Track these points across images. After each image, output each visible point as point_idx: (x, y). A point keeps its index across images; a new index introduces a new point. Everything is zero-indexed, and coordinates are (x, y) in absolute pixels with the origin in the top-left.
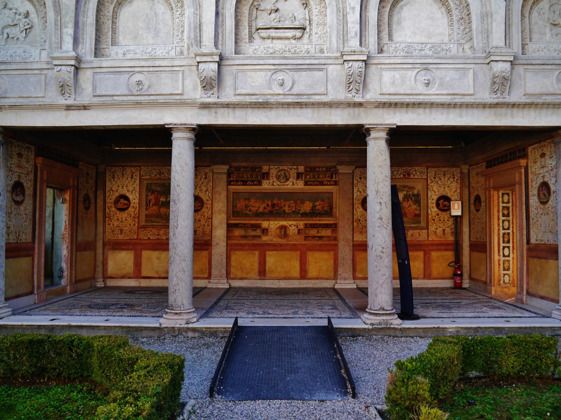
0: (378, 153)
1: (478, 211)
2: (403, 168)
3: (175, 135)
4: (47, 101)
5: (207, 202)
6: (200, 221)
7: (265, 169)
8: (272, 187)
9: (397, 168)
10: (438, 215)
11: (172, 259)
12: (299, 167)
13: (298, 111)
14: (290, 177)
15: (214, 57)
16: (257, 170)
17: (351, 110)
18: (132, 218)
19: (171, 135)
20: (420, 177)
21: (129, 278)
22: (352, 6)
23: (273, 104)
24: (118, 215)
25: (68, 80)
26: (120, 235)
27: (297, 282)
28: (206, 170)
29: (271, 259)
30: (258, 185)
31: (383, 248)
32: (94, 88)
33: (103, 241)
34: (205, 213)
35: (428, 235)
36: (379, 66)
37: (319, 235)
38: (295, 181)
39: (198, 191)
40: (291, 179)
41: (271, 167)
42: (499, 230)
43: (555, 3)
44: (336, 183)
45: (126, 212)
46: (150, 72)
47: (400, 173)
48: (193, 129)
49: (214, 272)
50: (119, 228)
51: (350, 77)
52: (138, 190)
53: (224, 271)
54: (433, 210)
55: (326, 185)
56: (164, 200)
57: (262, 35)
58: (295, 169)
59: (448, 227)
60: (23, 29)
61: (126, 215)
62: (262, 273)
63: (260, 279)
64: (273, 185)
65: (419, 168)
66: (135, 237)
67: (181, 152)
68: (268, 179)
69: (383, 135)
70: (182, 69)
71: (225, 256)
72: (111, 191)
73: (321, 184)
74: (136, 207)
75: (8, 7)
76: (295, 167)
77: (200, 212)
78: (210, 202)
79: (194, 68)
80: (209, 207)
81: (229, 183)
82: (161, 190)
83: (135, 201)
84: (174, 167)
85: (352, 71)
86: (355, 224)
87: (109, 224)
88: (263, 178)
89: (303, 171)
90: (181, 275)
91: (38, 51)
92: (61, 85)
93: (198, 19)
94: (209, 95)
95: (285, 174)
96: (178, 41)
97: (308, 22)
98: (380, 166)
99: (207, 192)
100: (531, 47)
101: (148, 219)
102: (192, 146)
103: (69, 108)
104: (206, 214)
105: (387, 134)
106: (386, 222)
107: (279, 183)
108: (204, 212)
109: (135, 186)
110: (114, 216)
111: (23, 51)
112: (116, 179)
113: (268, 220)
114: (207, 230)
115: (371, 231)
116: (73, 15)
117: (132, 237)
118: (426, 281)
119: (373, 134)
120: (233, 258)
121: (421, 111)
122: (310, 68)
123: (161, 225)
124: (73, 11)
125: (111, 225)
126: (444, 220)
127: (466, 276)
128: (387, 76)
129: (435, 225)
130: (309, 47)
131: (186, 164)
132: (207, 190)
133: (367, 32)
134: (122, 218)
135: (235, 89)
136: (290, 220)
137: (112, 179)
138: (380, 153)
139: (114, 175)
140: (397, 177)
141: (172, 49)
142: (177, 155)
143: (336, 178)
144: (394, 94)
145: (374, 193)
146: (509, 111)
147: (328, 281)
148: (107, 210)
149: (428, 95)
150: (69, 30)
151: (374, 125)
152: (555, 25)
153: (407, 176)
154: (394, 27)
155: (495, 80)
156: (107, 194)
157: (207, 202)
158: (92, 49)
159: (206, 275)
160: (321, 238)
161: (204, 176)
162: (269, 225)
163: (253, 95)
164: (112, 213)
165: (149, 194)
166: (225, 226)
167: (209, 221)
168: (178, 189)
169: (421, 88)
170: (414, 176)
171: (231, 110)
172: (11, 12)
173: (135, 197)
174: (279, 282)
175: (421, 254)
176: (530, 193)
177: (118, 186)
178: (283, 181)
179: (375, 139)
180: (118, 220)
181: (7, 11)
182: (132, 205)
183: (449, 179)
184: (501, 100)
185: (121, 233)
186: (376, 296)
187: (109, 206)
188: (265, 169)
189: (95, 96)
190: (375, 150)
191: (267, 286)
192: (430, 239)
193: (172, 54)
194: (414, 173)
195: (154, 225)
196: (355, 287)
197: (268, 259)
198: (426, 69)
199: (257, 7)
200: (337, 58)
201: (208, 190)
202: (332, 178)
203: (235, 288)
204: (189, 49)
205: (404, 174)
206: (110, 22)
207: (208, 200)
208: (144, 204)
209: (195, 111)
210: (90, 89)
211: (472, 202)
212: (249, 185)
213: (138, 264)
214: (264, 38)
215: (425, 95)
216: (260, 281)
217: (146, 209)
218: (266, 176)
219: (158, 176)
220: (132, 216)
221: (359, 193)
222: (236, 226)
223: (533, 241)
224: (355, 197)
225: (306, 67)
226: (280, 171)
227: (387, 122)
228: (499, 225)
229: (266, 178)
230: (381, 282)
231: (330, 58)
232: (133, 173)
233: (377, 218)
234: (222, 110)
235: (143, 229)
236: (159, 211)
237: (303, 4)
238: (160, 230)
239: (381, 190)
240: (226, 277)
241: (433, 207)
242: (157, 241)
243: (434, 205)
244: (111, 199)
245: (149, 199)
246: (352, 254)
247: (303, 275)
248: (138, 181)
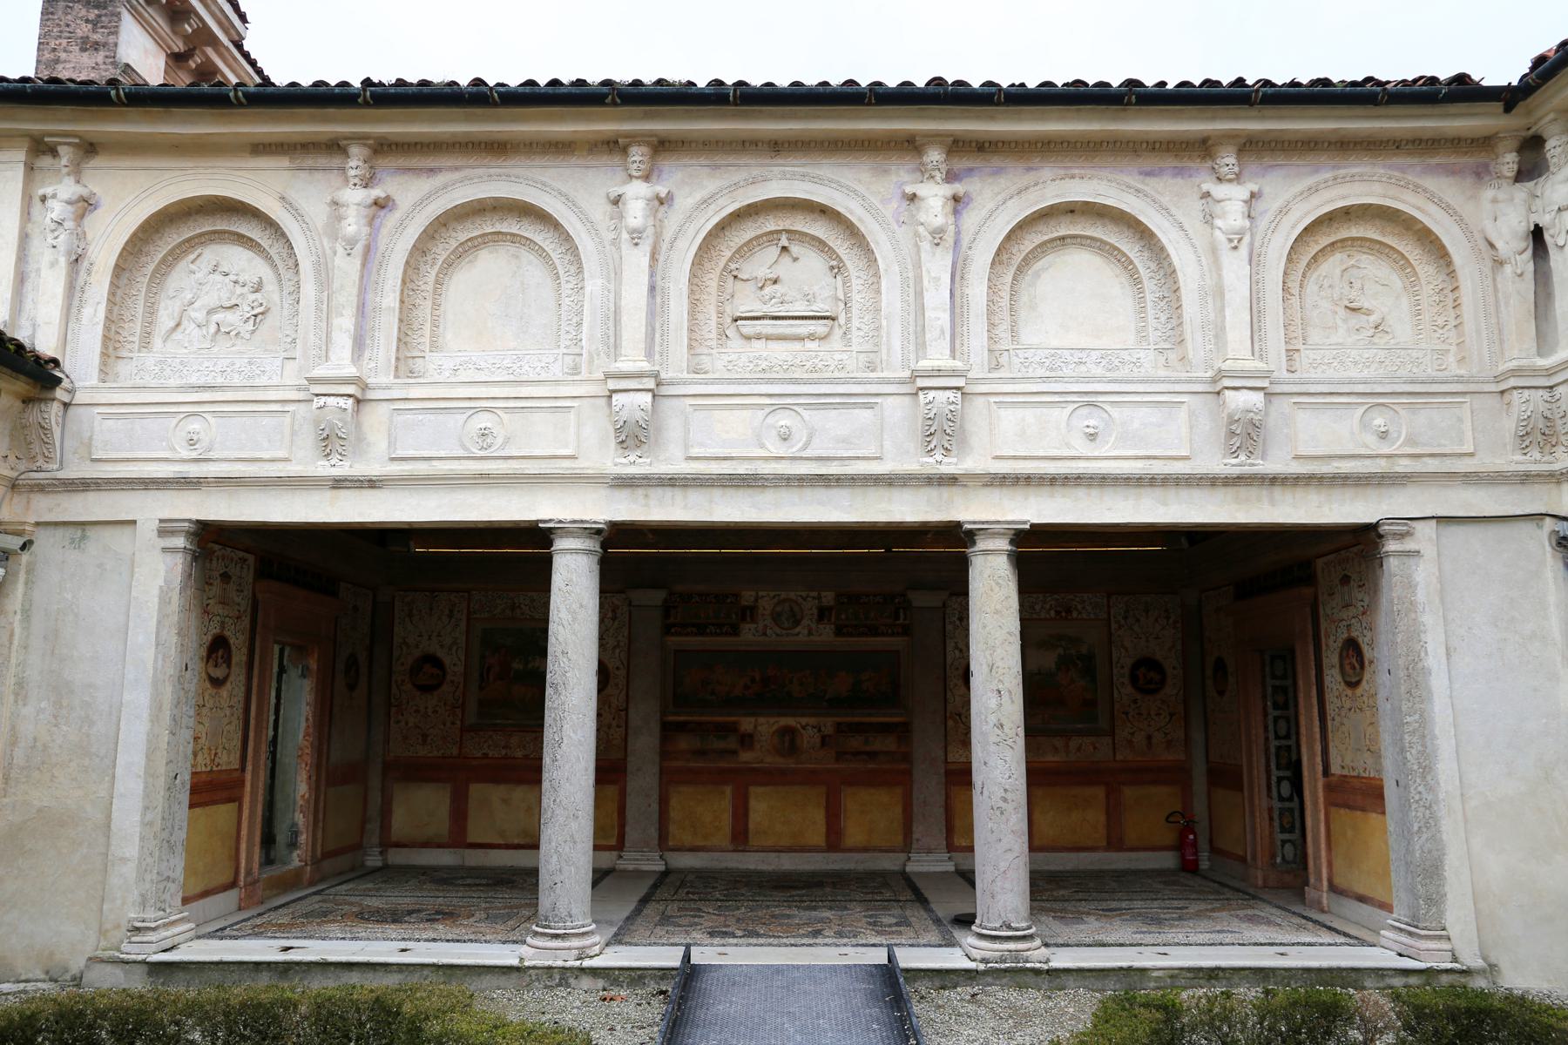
0: (993, 584)
1: (1221, 693)
2: (1056, 596)
3: (560, 544)
4: (293, 469)
5: (617, 672)
7: (748, 597)
8: (762, 638)
9: (1041, 596)
10: (1135, 701)
11: (549, 814)
12: (823, 594)
13: (821, 493)
14: (802, 618)
15: (645, 380)
16: (729, 600)
17: (933, 492)
19: (550, 544)
20: (1092, 616)
21: (440, 846)
22: (933, 275)
23: (766, 479)
25: (340, 425)
27: (818, 857)
29: (761, 806)
30: (731, 635)
31: (1006, 790)
32: (392, 443)
35: (1114, 749)
36: (993, 399)
37: (868, 749)
38: (814, 626)
40: (805, 622)
41: (761, 594)
42: (1267, 739)
43: (1353, 266)
44: (906, 631)
46: (507, 410)
47: (1048, 606)
48: (598, 532)
49: (632, 835)
51: (930, 422)
52: (464, 645)
53: (653, 832)
54: (1125, 691)
55: (883, 634)
56: (521, 667)
57: (745, 331)
58: (814, 598)
59: (1158, 730)
60: (249, 315)
62: (740, 838)
63: (734, 851)
64: (765, 634)
65: (1090, 596)
66: (455, 751)
67: (571, 580)
68: (753, 620)
69: (1003, 544)
70: (575, 403)
71: (655, 797)
73: (873, 631)
75: (219, 270)
76: (814, 594)
78: (623, 672)
79: (603, 401)
81: (667, 630)
84: (555, 612)
85: (934, 411)
86: (950, 723)
88: (743, 619)
89: (832, 603)
90: (567, 849)
91: (278, 362)
92: (325, 435)
93: (612, 300)
94: (632, 458)
95: (792, 610)
96: (568, 343)
97: (842, 305)
98: (997, 612)
99: (617, 651)
100: (1306, 357)
102: (596, 568)
103: (338, 484)
105: (1012, 542)
106: (1011, 733)
107: (778, 631)
111: (246, 361)
113: (753, 715)
115: (980, 755)
116: (355, 291)
118: (1114, 855)
119: (982, 544)
120: (674, 802)
121: (1081, 492)
122: (847, 402)
124: (354, 283)
126: (1149, 714)
127: (1203, 844)
128: (1009, 419)
129: (1129, 725)
130: (845, 356)
131: (581, 606)
132: (618, 646)
133: (965, 328)
134: (426, 708)
135: (686, 447)
136: (803, 715)
138: (998, 584)
140: (1043, 615)
141: (556, 360)
142: (562, 586)
143: (905, 619)
144: (1025, 458)
145: (985, 669)
146: (1264, 492)
147: (891, 854)
148: (394, 690)
149: (1096, 458)
150: (345, 323)
151: (983, 523)
152: (1354, 310)
153: (1064, 614)
154: (1023, 314)
155: (1233, 427)
157: (617, 672)
158: (389, 360)
159: (613, 842)
160: (872, 755)
161: (610, 615)
162: (755, 727)
163: (725, 459)
166: (655, 727)
168: (563, 660)
169: (1081, 447)
170: (1080, 613)
171: (678, 493)
172: (227, 279)
174: (778, 857)
175: (1099, 792)
176: (1325, 661)
177: (420, 636)
178: (786, 625)
179: (986, 552)
180: (417, 711)
181: (218, 277)
182: (449, 678)
183: (1156, 620)
184: (1246, 470)
185: (424, 742)
186: (993, 897)
188: (748, 597)
189: (393, 459)
190: (986, 576)
191: (752, 867)
192: (1119, 757)
193: (556, 371)
194: (1079, 607)
196: (953, 869)
197: (753, 803)
198: (1090, 404)
199: (735, 273)
200: (902, 382)
202: (897, 618)
203: (680, 871)
204: (591, 361)
205: (1058, 609)
206: (429, 303)
207: (618, 668)
209: (603, 492)
210: (383, 445)
211: (1209, 672)
212: (711, 634)
213: (459, 815)
214: (748, 338)
215: (1088, 458)
216: (735, 856)
218: (749, 613)
221: (957, 652)
222: (682, 727)
223: (1335, 769)
224: (949, 660)
225: (838, 400)
226: (780, 602)
227: (1010, 518)
228: (1266, 728)
229: (748, 619)
230: (1003, 865)
231: (889, 382)
233: (992, 725)
234: (660, 491)
235: (472, 734)
237: (832, 268)
239: (1000, 664)
240: (659, 845)
241: (1123, 683)
243: (1126, 680)
244: (403, 664)
246: (944, 792)
247: (834, 842)
248: (463, 625)
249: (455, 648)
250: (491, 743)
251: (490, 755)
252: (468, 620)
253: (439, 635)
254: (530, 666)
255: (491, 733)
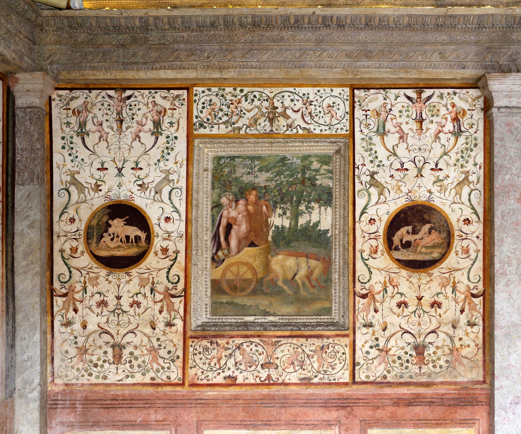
5: (466, 228)
6: (439, 305)
18: (159, 297)
24: (103, 285)
26: (113, 367)
28: (456, 100)
33: (44, 396)
34: (458, 275)
39: (430, 186)
45: (134, 271)
50: (106, 337)
52: (183, 184)
56: (287, 223)
61: (134, 286)
66: (175, 375)
72: (73, 189)
74: (177, 252)
77: (436, 271)
80: (472, 248)
82: (272, 184)
83: (169, 227)
87: (68, 324)
99: (466, 190)
101: (224, 299)
104: (461, 277)
108: (452, 270)
109: (170, 165)
110: (85, 289)
112: (90, 141)
114: (466, 341)
117: (162, 377)
123: (274, 325)
125: (77, 326)
132: (466, 181)
134: (119, 298)
137: (77, 140)
139: (82, 125)
148: (59, 267)
156: (59, 202)
157: (466, 228)
161: (449, 126)
164: (76, 275)
165: (224, 200)
167: (473, 308)
173: (169, 211)
180: (103, 304)
182: (158, 243)
185: (118, 358)
187: (67, 247)
195: (246, 325)
201: (466, 178)
207: (467, 221)
208: (207, 237)
217: (216, 261)
219: (264, 125)
220: (160, 288)
232: (162, 112)
235: (205, 343)
236: (267, 265)
238: (275, 345)
242: (265, 391)
244: (72, 220)
245: (224, 222)
248: (181, 146)
249: (166, 190)
250: (239, 358)
251: (240, 380)
252: (190, 138)
253: (136, 168)
254: (302, 221)
255: (238, 341)
